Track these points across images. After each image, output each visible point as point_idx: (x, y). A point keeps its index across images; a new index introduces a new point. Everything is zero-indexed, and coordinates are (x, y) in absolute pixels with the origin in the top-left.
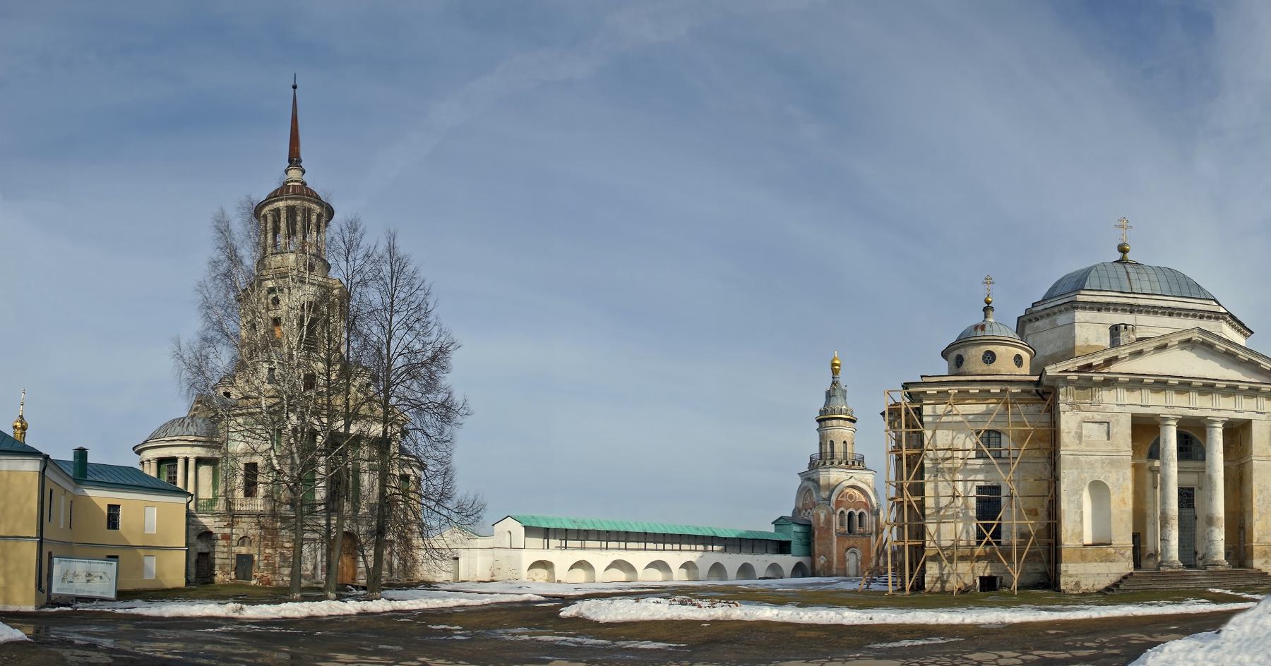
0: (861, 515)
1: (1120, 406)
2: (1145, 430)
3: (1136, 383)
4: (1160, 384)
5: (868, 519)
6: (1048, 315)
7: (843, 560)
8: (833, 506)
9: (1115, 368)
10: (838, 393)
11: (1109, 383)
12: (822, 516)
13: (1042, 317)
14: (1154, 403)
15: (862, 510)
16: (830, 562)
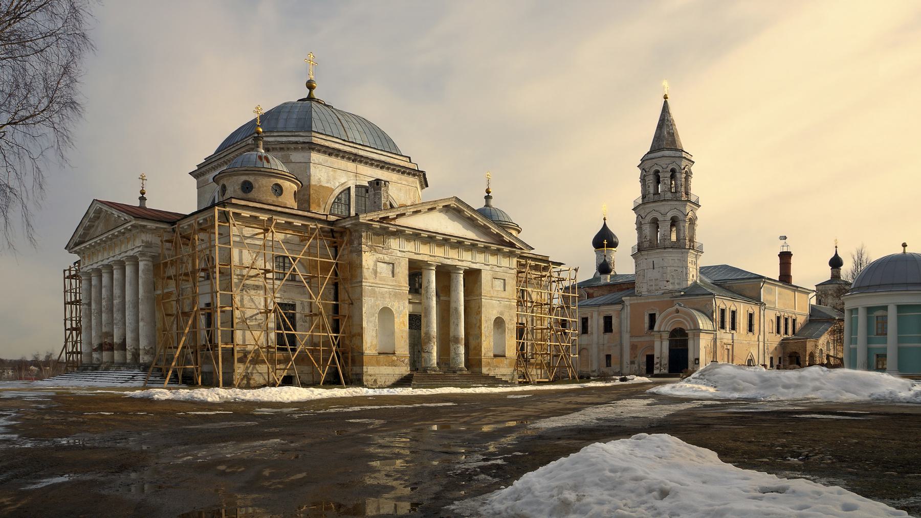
1: (402, 251)
2: (416, 271)
3: (416, 236)
4: (431, 238)
6: (282, 149)
9: (401, 221)
11: (399, 233)
13: (274, 149)
14: (424, 253)
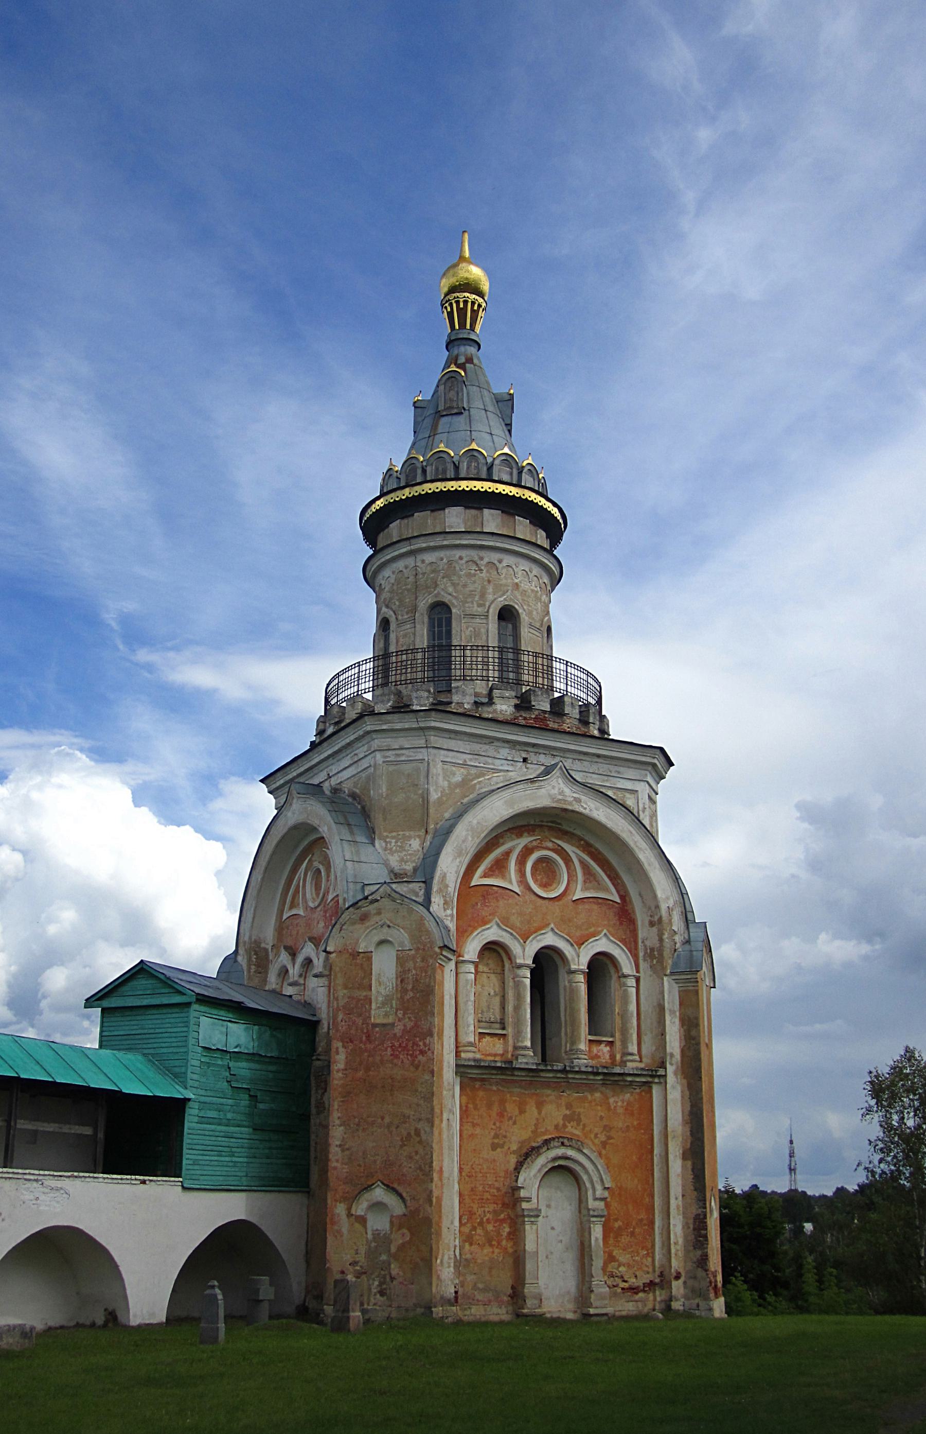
0: (600, 966)
5: (640, 991)
7: (512, 1209)
8: (443, 909)
10: (477, 401)
12: (385, 967)
15: (602, 944)
16: (419, 1225)
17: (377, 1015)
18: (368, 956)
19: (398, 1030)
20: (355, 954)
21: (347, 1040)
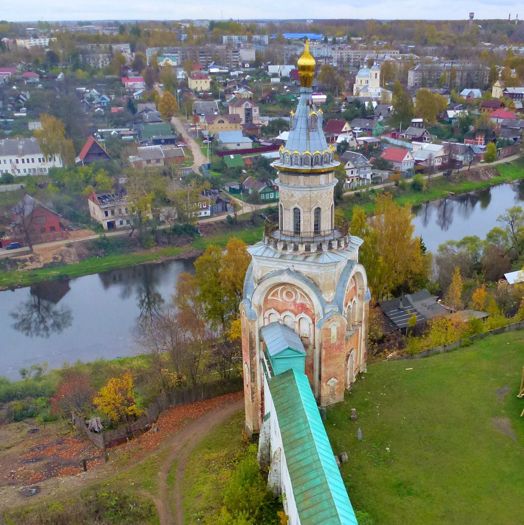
17: (332, 342)
18: (330, 329)
19: (337, 344)
20: (327, 329)
21: (325, 348)
